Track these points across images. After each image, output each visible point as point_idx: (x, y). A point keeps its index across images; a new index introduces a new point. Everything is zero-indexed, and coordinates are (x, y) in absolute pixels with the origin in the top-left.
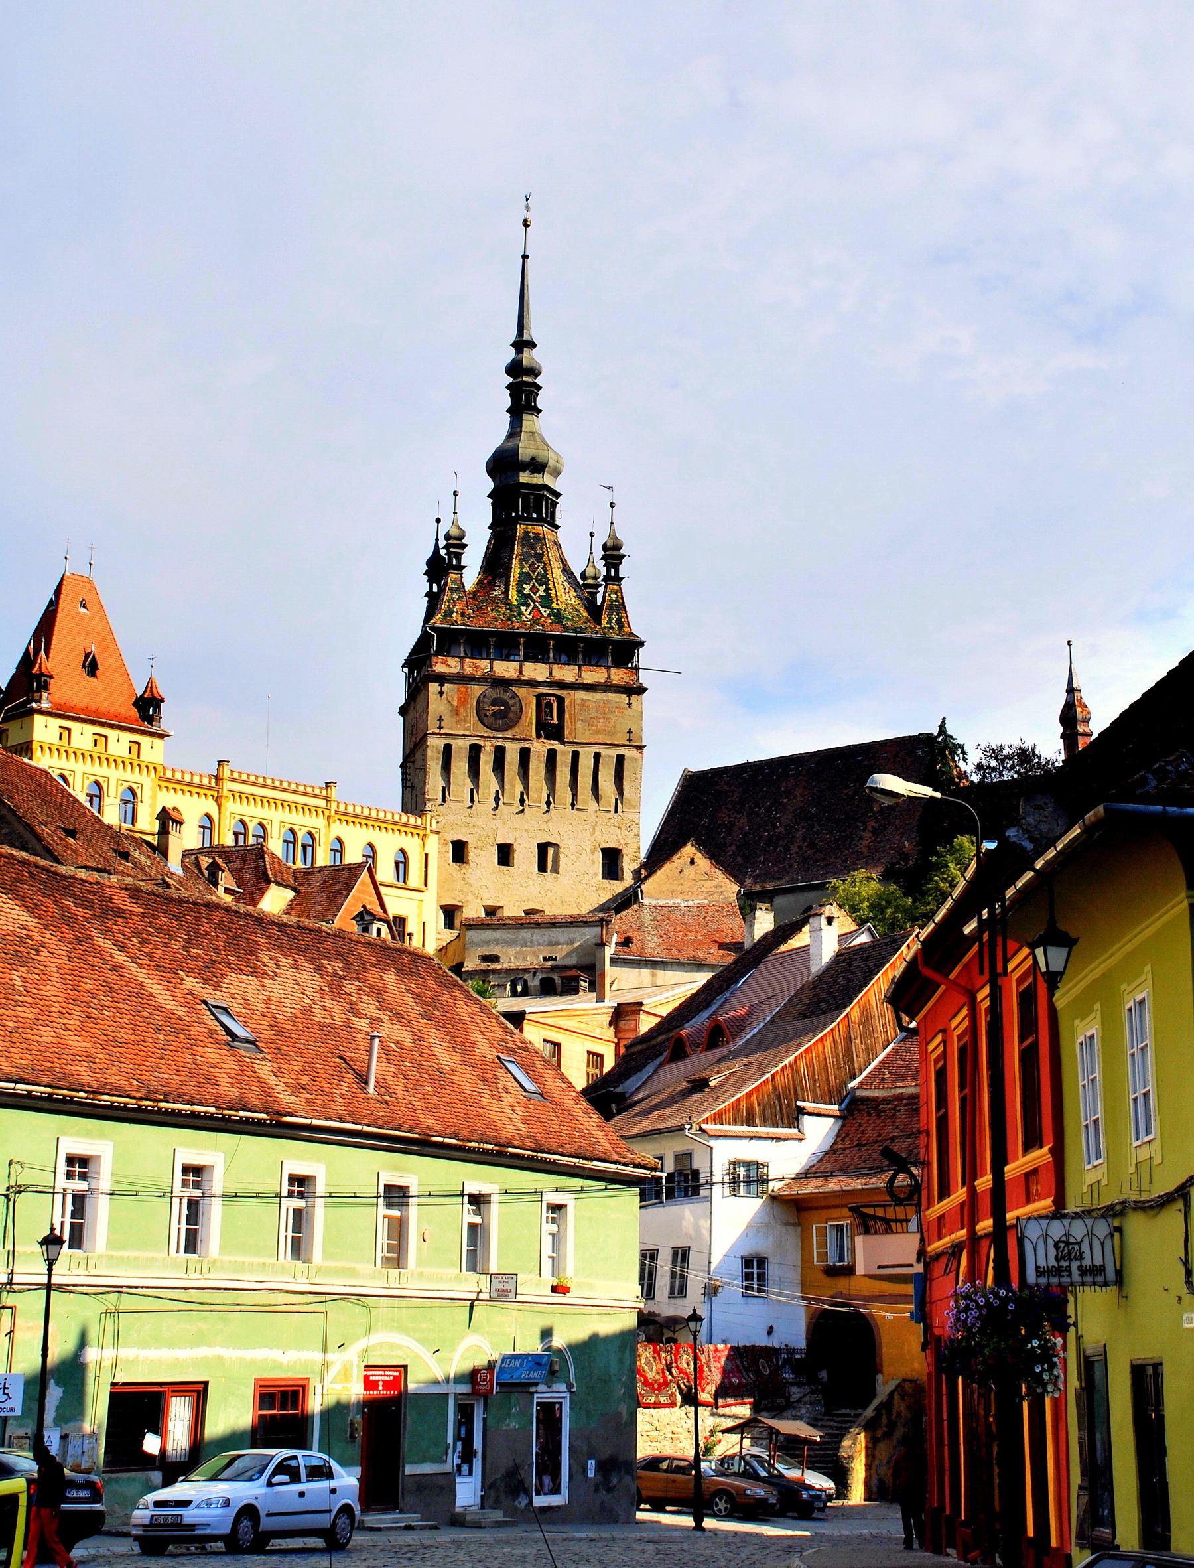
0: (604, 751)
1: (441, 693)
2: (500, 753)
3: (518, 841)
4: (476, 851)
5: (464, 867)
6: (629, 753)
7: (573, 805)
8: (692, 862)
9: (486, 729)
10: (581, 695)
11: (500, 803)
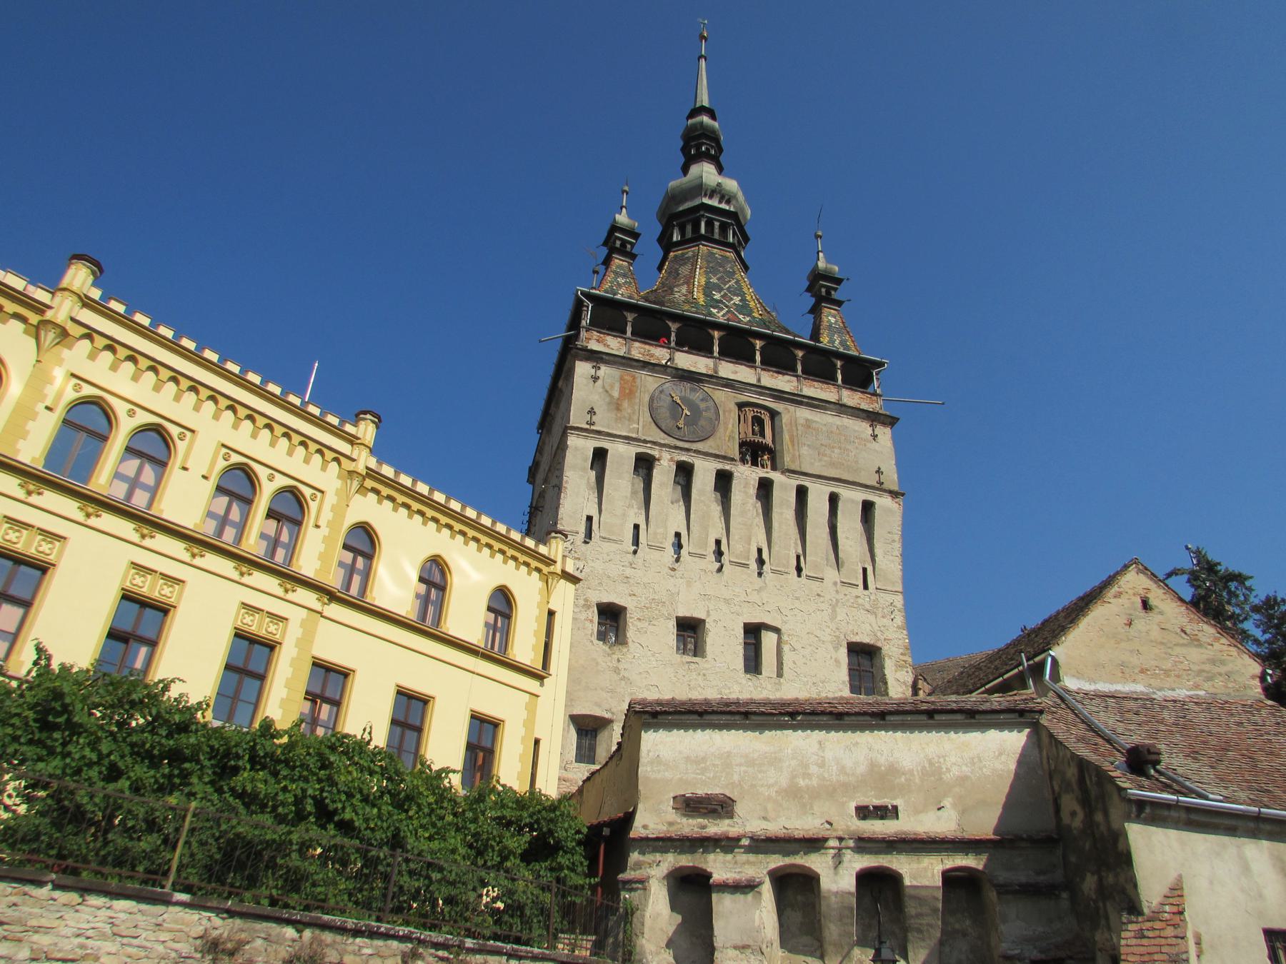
0: (845, 493)
1: (595, 379)
2: (685, 472)
3: (714, 615)
4: (639, 624)
5: (619, 652)
6: (883, 503)
7: (799, 570)
8: (1146, 605)
9: (663, 435)
10: (803, 413)
11: (682, 551)
